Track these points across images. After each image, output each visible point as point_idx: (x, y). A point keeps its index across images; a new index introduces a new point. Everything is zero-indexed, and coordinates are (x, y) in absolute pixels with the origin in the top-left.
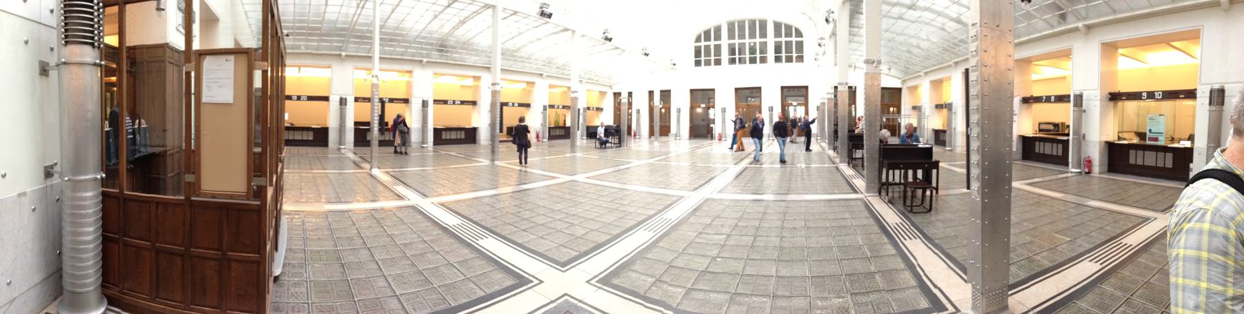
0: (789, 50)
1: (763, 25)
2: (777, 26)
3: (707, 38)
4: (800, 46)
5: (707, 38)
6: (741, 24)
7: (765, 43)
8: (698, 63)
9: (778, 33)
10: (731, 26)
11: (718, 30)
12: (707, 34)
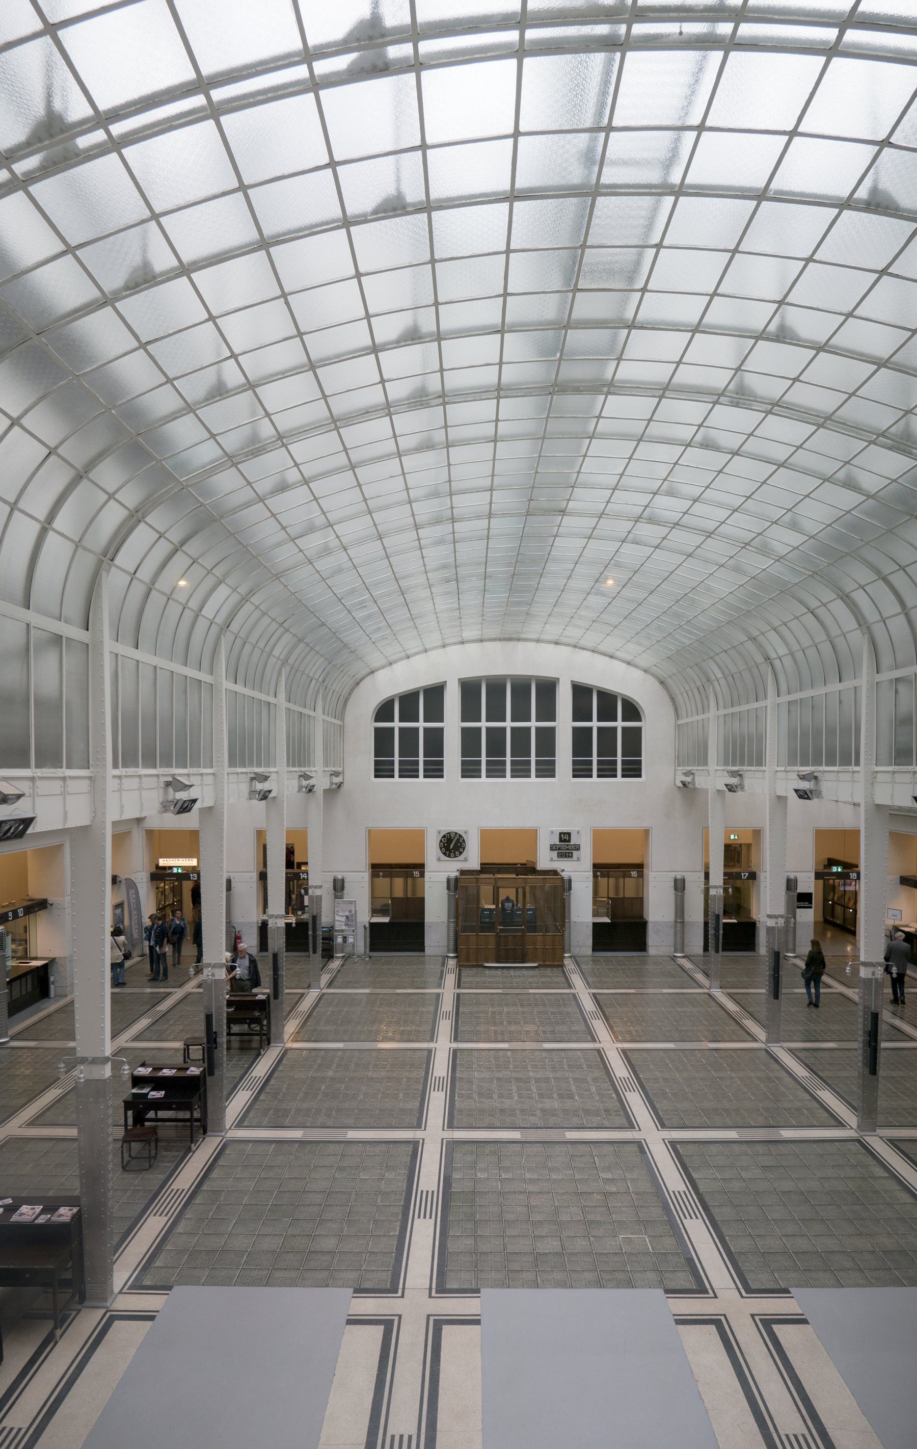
0: (607, 747)
1: (548, 688)
2: (581, 692)
3: (409, 713)
4: (633, 739)
5: (409, 713)
6: (496, 686)
7: (552, 730)
8: (382, 770)
9: (581, 712)
10: (469, 689)
11: (435, 694)
12: (408, 701)
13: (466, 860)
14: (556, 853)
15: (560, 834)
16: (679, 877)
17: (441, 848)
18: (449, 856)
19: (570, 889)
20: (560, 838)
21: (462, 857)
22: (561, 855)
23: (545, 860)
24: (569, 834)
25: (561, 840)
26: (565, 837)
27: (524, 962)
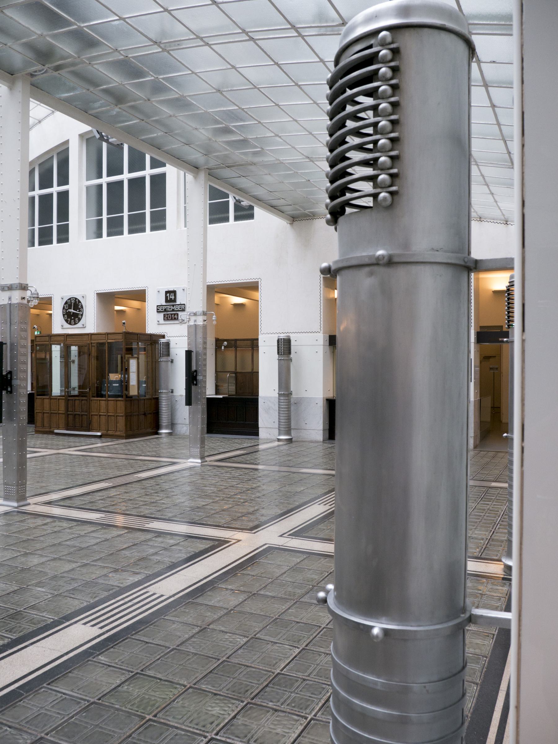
13: (84, 327)
14: (162, 315)
15: (167, 292)
16: (282, 336)
17: (64, 315)
18: (70, 324)
19: (168, 354)
20: (166, 297)
21: (80, 325)
22: (166, 318)
23: (154, 324)
24: (174, 292)
25: (167, 301)
26: (171, 296)
27: (89, 431)
